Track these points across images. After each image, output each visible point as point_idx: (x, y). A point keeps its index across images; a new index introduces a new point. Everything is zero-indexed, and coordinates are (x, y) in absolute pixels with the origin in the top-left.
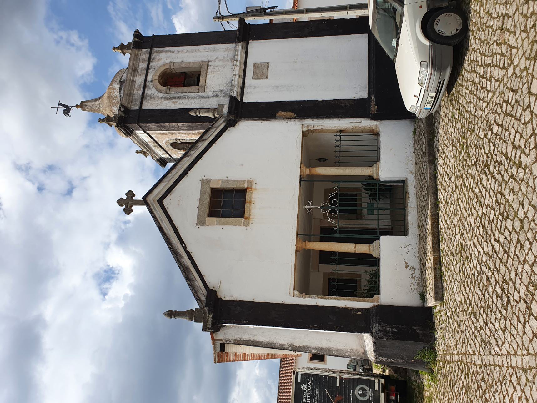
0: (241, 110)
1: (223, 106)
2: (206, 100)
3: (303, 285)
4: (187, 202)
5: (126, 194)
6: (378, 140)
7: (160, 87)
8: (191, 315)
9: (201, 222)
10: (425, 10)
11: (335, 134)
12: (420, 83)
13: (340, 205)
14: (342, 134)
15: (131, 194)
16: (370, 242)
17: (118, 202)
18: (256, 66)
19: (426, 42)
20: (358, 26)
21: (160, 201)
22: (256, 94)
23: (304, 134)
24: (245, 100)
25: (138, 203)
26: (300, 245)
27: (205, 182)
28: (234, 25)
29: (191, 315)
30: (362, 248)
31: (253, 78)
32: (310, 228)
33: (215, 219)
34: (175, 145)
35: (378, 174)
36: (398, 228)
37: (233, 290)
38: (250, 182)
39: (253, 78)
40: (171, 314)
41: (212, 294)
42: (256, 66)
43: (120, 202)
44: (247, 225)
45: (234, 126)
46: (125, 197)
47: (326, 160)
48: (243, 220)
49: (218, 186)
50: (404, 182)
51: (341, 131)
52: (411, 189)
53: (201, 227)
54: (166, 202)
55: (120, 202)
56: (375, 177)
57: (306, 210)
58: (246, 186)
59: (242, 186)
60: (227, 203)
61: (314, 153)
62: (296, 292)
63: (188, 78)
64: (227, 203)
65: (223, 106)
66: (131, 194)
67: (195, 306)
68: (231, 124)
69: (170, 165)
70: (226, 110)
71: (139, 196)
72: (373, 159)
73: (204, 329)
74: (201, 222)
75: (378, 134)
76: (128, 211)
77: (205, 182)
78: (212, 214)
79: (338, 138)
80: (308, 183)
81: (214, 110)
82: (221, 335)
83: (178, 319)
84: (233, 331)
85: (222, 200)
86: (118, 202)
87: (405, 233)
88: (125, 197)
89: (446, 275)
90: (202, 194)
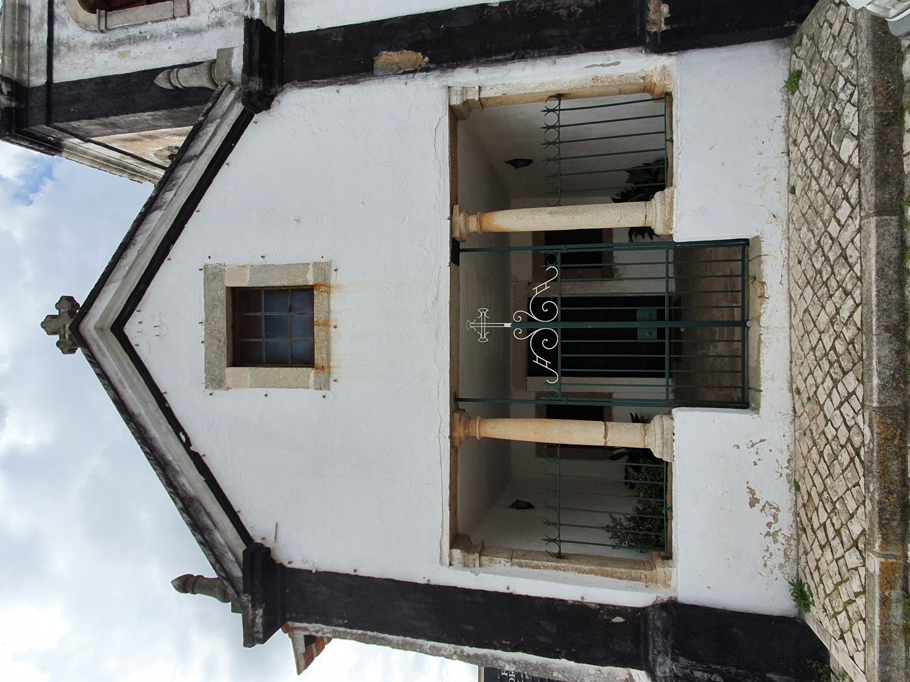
2: (196, 38)
4: (177, 327)
5: (58, 306)
6: (668, 116)
7: (83, 14)
9: (215, 382)
11: (543, 106)
13: (565, 317)
14: (565, 104)
17: (44, 325)
23: (456, 115)
24: (292, 26)
26: (460, 433)
27: (212, 274)
32: (483, 383)
33: (246, 372)
35: (668, 223)
37: (307, 547)
38: (323, 268)
44: (323, 386)
45: (267, 106)
47: (528, 162)
48: (311, 372)
51: (559, 96)
52: (774, 272)
53: (218, 393)
54: (131, 329)
56: (659, 229)
58: (310, 279)
59: (300, 282)
60: (268, 326)
61: (493, 162)
64: (268, 326)
68: (258, 102)
70: (237, 63)
72: (649, 178)
73: (252, 638)
74: (215, 382)
75: (667, 98)
77: (212, 274)
85: (262, 314)
90: (209, 307)
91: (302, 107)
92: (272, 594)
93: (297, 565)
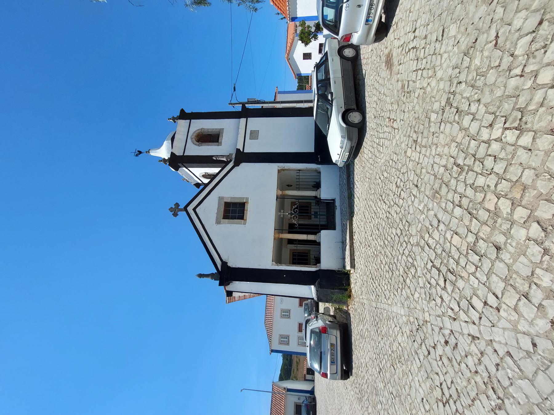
0: (242, 157)
1: (232, 154)
3: (278, 259)
4: (209, 210)
5: (175, 205)
6: (320, 176)
7: (195, 142)
8: (212, 276)
9: (218, 222)
10: (343, 109)
12: (342, 147)
13: (299, 213)
15: (177, 205)
16: (315, 233)
17: (169, 209)
18: (252, 132)
19: (344, 126)
20: (308, 112)
21: (194, 210)
22: (252, 147)
23: (279, 171)
24: (246, 151)
25: (181, 210)
26: (277, 236)
27: (220, 199)
28: (239, 108)
29: (212, 276)
30: (311, 237)
31: (250, 139)
32: (283, 225)
34: (205, 176)
35: (320, 195)
36: (330, 226)
38: (247, 199)
39: (250, 139)
40: (201, 276)
41: (224, 264)
42: (252, 132)
43: (171, 209)
46: (174, 207)
47: (291, 186)
49: (229, 201)
50: (334, 200)
51: (299, 170)
52: (337, 204)
54: (197, 210)
55: (171, 209)
57: (280, 215)
59: (242, 201)
60: (234, 211)
61: (284, 183)
62: (274, 263)
63: (212, 138)
64: (234, 211)
65: (232, 154)
66: (177, 205)
67: (215, 271)
68: (237, 164)
69: (201, 187)
70: (234, 156)
71: (182, 207)
72: (317, 186)
73: (220, 285)
74: (218, 222)
75: (320, 173)
76: (175, 215)
77: (220, 199)
78: (226, 217)
79: (298, 174)
80: (281, 199)
81: (227, 157)
82: (230, 288)
83: (205, 279)
84: (237, 286)
86: (169, 209)
87: (334, 229)
88: (174, 207)
89: (357, 254)
91: (244, 166)
92: (227, 275)
93: (234, 266)
